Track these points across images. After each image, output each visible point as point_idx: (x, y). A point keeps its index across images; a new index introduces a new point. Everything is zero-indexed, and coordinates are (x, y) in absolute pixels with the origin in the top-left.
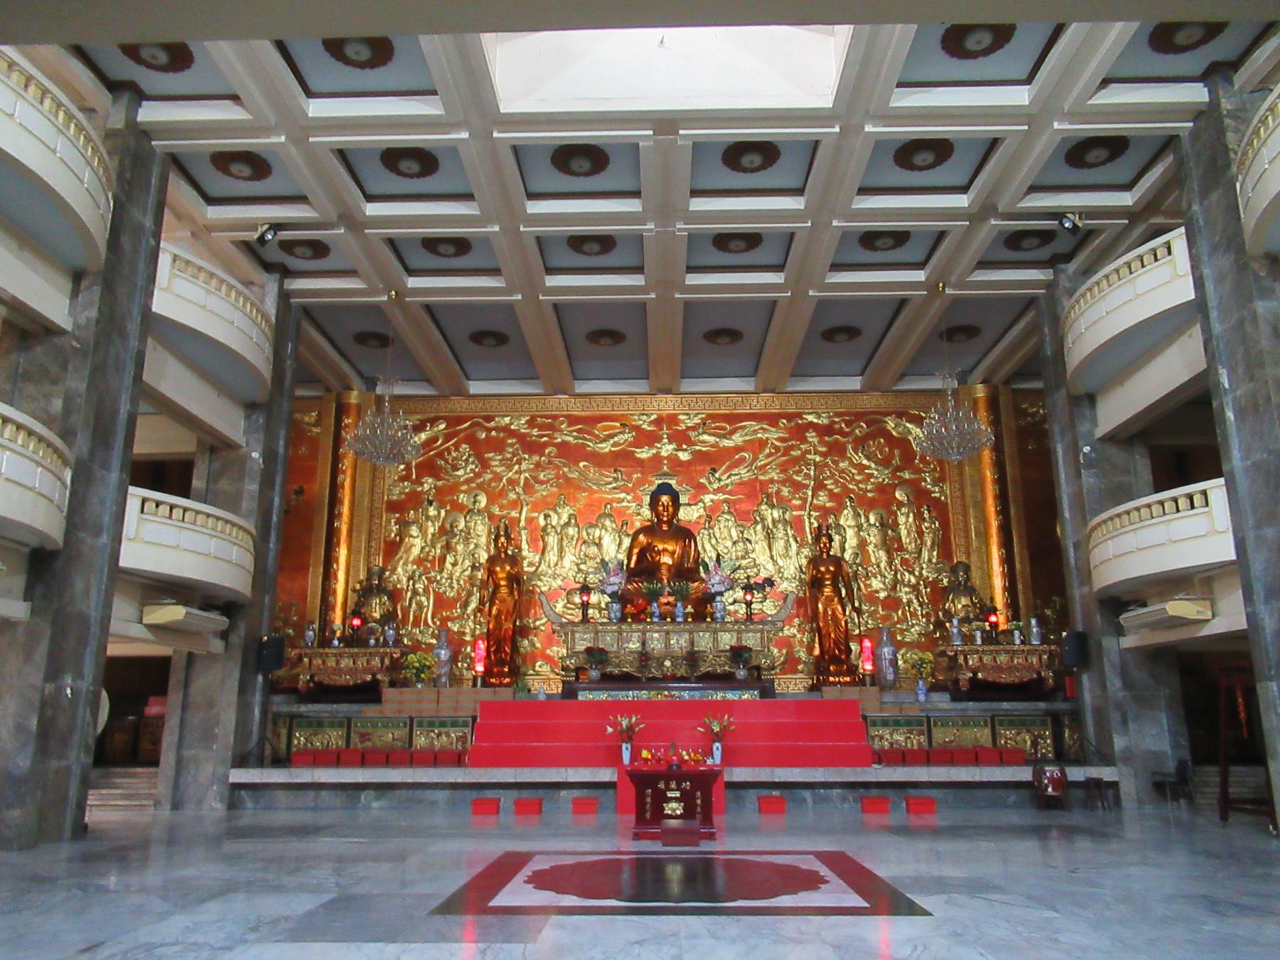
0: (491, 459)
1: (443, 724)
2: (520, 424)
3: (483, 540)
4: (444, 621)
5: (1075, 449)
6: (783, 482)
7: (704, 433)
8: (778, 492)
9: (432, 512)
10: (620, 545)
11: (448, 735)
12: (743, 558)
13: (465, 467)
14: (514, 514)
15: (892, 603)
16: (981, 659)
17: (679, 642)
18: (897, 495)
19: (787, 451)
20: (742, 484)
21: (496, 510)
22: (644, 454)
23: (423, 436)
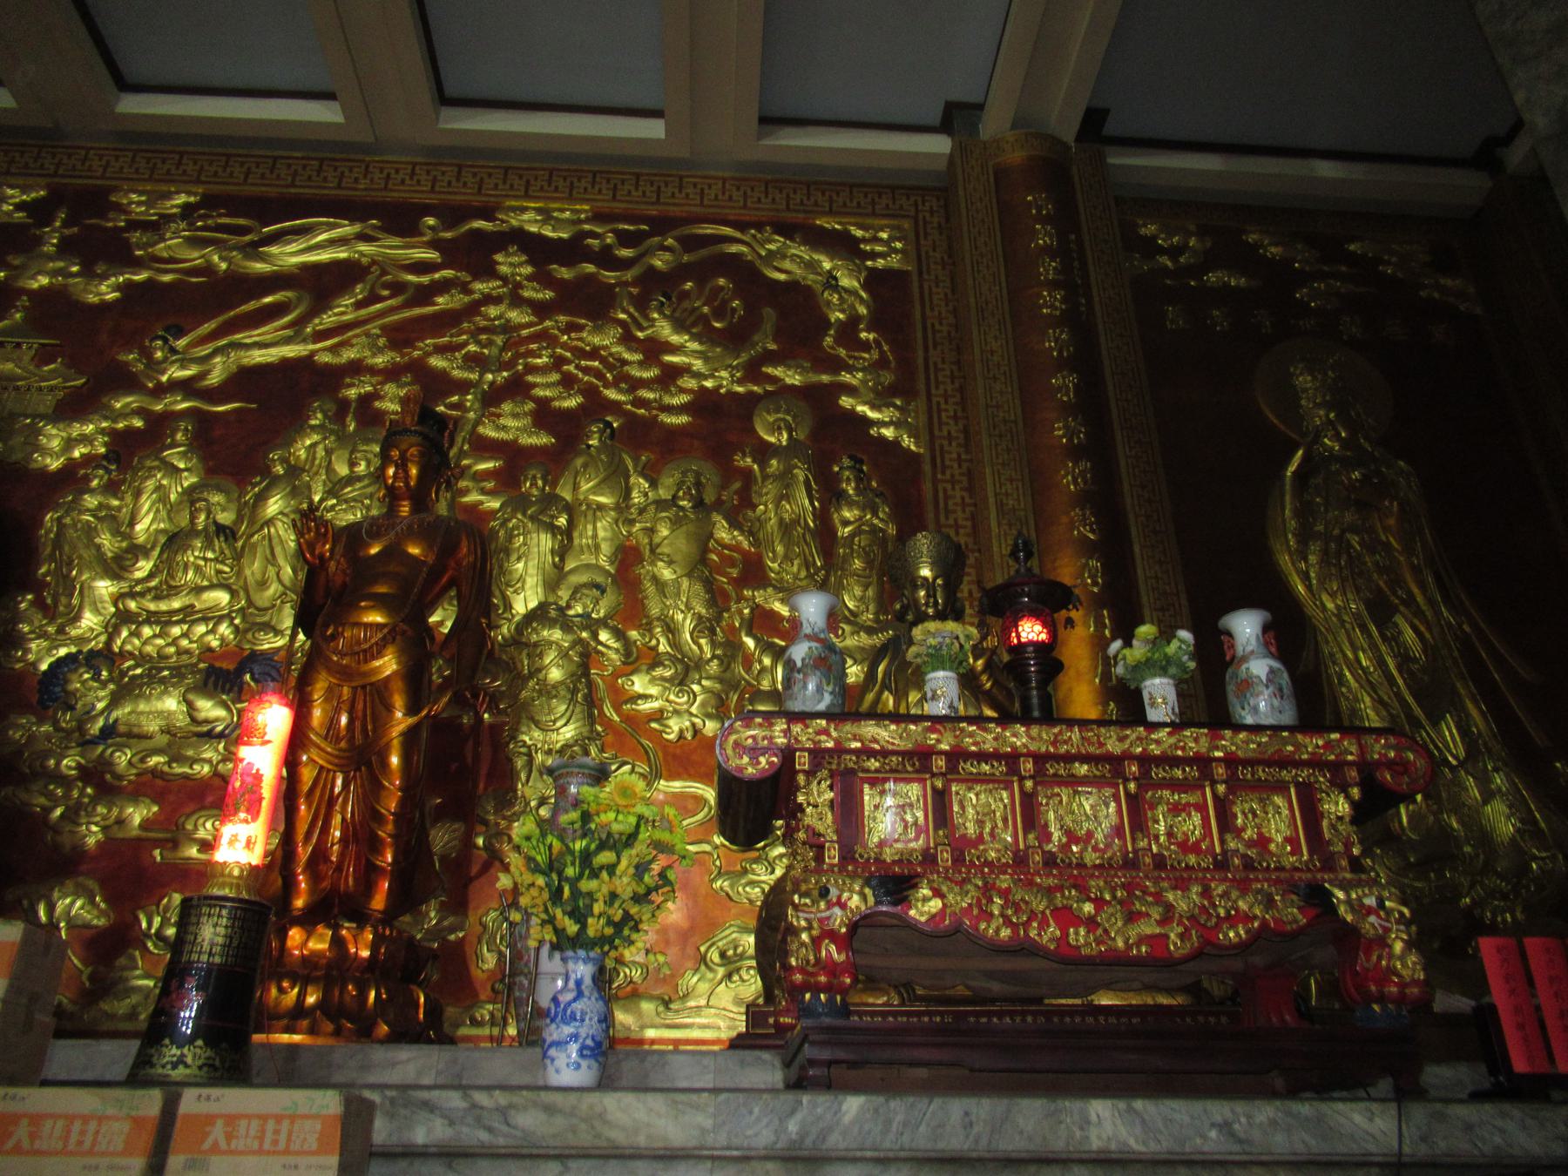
6: (391, 374)
19: (424, 295)
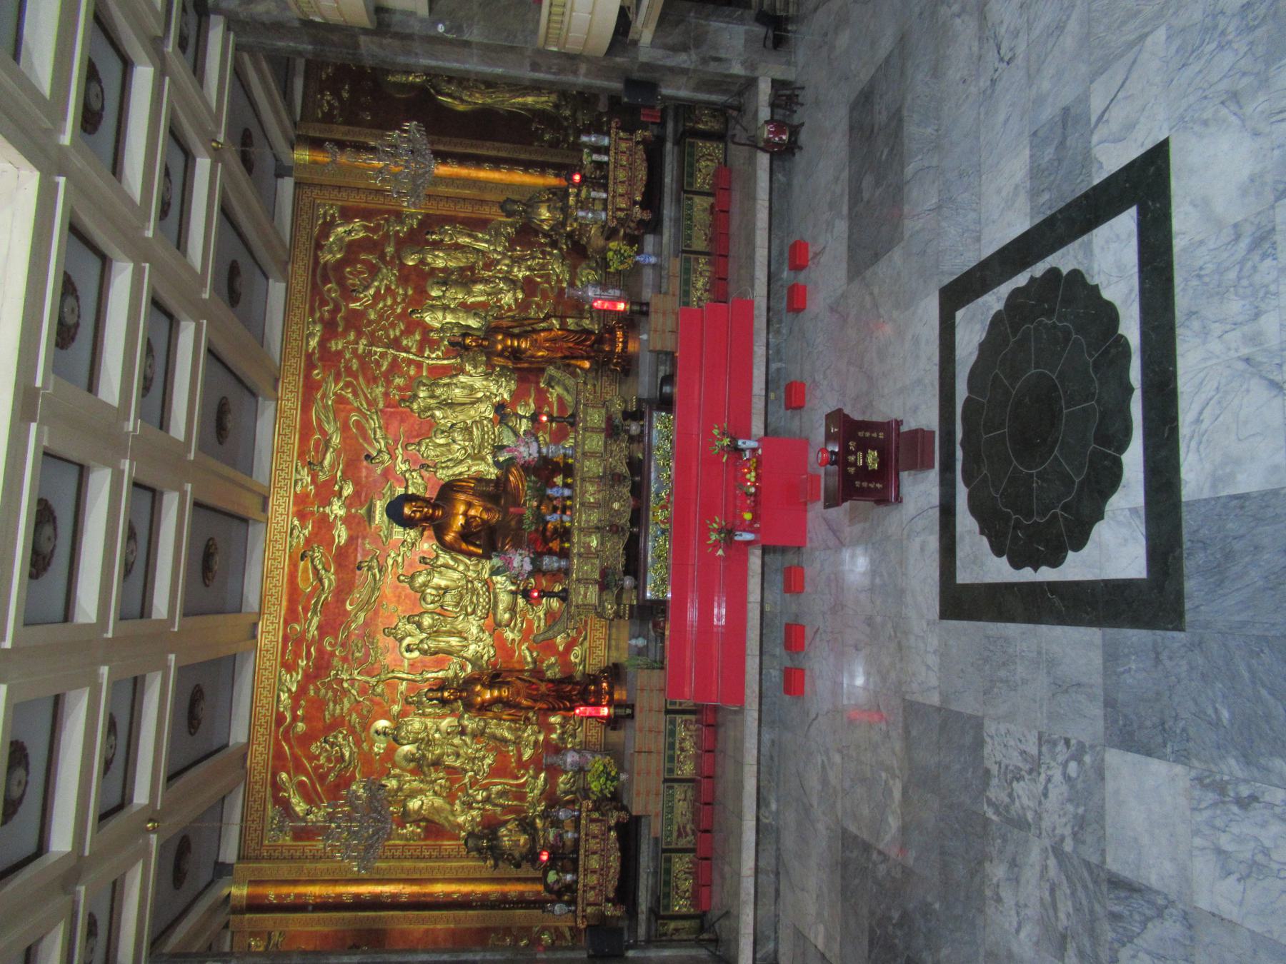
0: (333, 716)
1: (672, 746)
2: (292, 682)
3: (429, 722)
4: (522, 765)
5: (439, 40)
6: (389, 383)
7: (321, 463)
8: (399, 388)
9: (393, 784)
10: (447, 566)
11: (684, 740)
12: (471, 433)
13: (340, 746)
14: (403, 686)
15: (529, 286)
16: (622, 195)
17: (591, 493)
18: (411, 263)
20: (385, 428)
21: (396, 709)
22: (341, 534)
23: (295, 800)
